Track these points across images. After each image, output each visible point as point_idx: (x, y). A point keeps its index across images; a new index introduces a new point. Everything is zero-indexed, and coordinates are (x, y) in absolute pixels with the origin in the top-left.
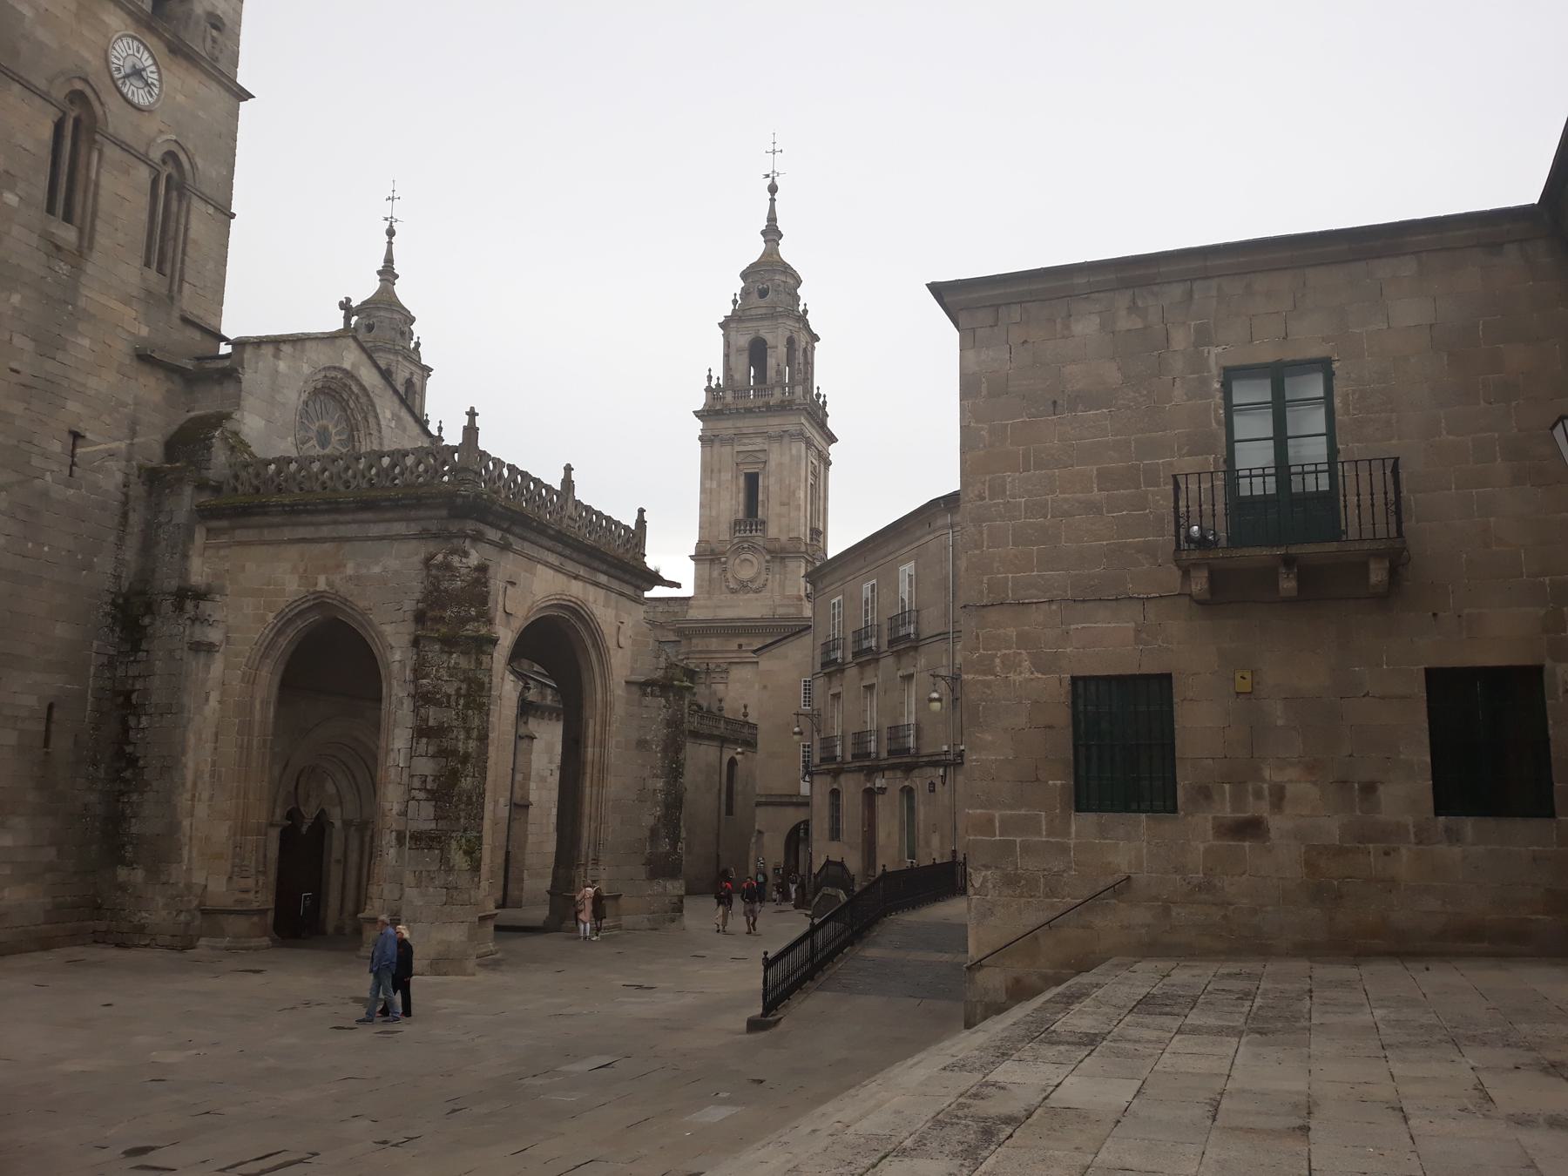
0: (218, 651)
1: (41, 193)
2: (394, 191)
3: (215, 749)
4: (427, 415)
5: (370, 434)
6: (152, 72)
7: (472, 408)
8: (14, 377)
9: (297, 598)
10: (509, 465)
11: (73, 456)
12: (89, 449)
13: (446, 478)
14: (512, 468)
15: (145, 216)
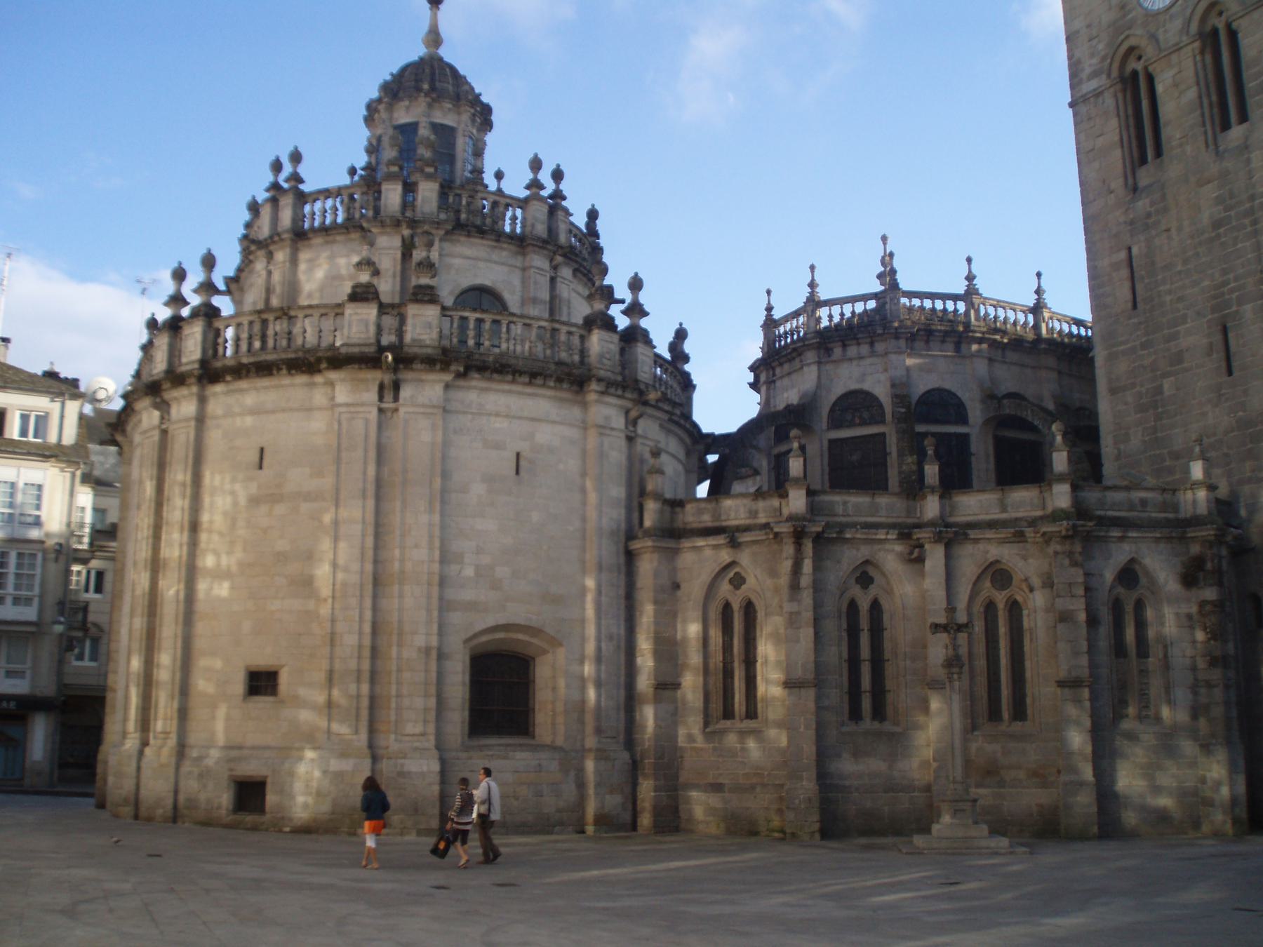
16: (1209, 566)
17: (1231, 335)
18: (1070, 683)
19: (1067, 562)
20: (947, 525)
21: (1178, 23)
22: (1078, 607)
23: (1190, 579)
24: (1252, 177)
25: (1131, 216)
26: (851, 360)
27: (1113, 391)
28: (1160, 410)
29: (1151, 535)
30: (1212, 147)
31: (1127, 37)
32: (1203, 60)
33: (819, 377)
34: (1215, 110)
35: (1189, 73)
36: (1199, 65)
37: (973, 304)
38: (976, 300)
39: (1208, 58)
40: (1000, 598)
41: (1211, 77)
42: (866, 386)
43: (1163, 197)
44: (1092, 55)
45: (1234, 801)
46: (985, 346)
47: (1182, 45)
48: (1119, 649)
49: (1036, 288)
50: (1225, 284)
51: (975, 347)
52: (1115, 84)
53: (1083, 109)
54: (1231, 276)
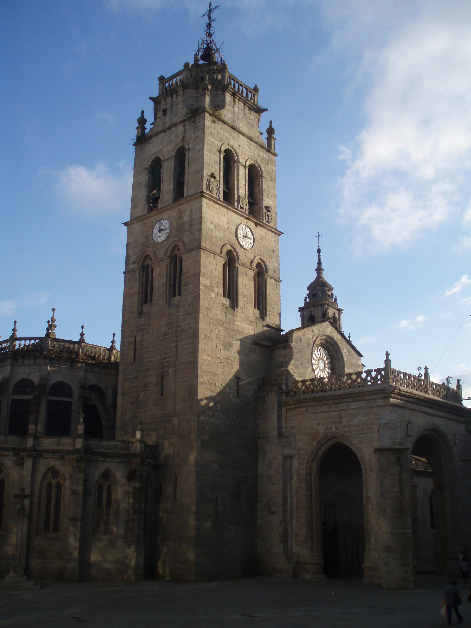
0: (295, 458)
1: (221, 291)
2: (318, 232)
3: (297, 498)
4: (343, 331)
5: (339, 360)
6: (250, 235)
7: (387, 352)
8: (218, 360)
9: (324, 435)
10: (403, 373)
11: (238, 386)
12: (243, 383)
13: (379, 382)
14: (405, 374)
15: (252, 290)
16: (137, 474)
17: (164, 379)
18: (73, 520)
19: (77, 470)
20: (35, 451)
21: (163, 250)
22: (80, 488)
23: (130, 478)
24: (179, 318)
25: (138, 324)
26: (25, 365)
27: (123, 394)
28: (138, 405)
29: (116, 460)
30: (168, 303)
31: (147, 250)
32: (170, 267)
33: (11, 371)
34: (172, 288)
35: (164, 271)
36: (168, 268)
37: (81, 346)
38: (83, 345)
39: (172, 267)
40: (54, 481)
41: (172, 274)
42: (30, 378)
43: (150, 318)
44: (134, 255)
45: (137, 566)
46: (84, 364)
47: (164, 259)
48: (99, 505)
49: (112, 340)
50: (165, 358)
51: (79, 365)
52: (140, 269)
53: (128, 276)
54: (167, 356)
